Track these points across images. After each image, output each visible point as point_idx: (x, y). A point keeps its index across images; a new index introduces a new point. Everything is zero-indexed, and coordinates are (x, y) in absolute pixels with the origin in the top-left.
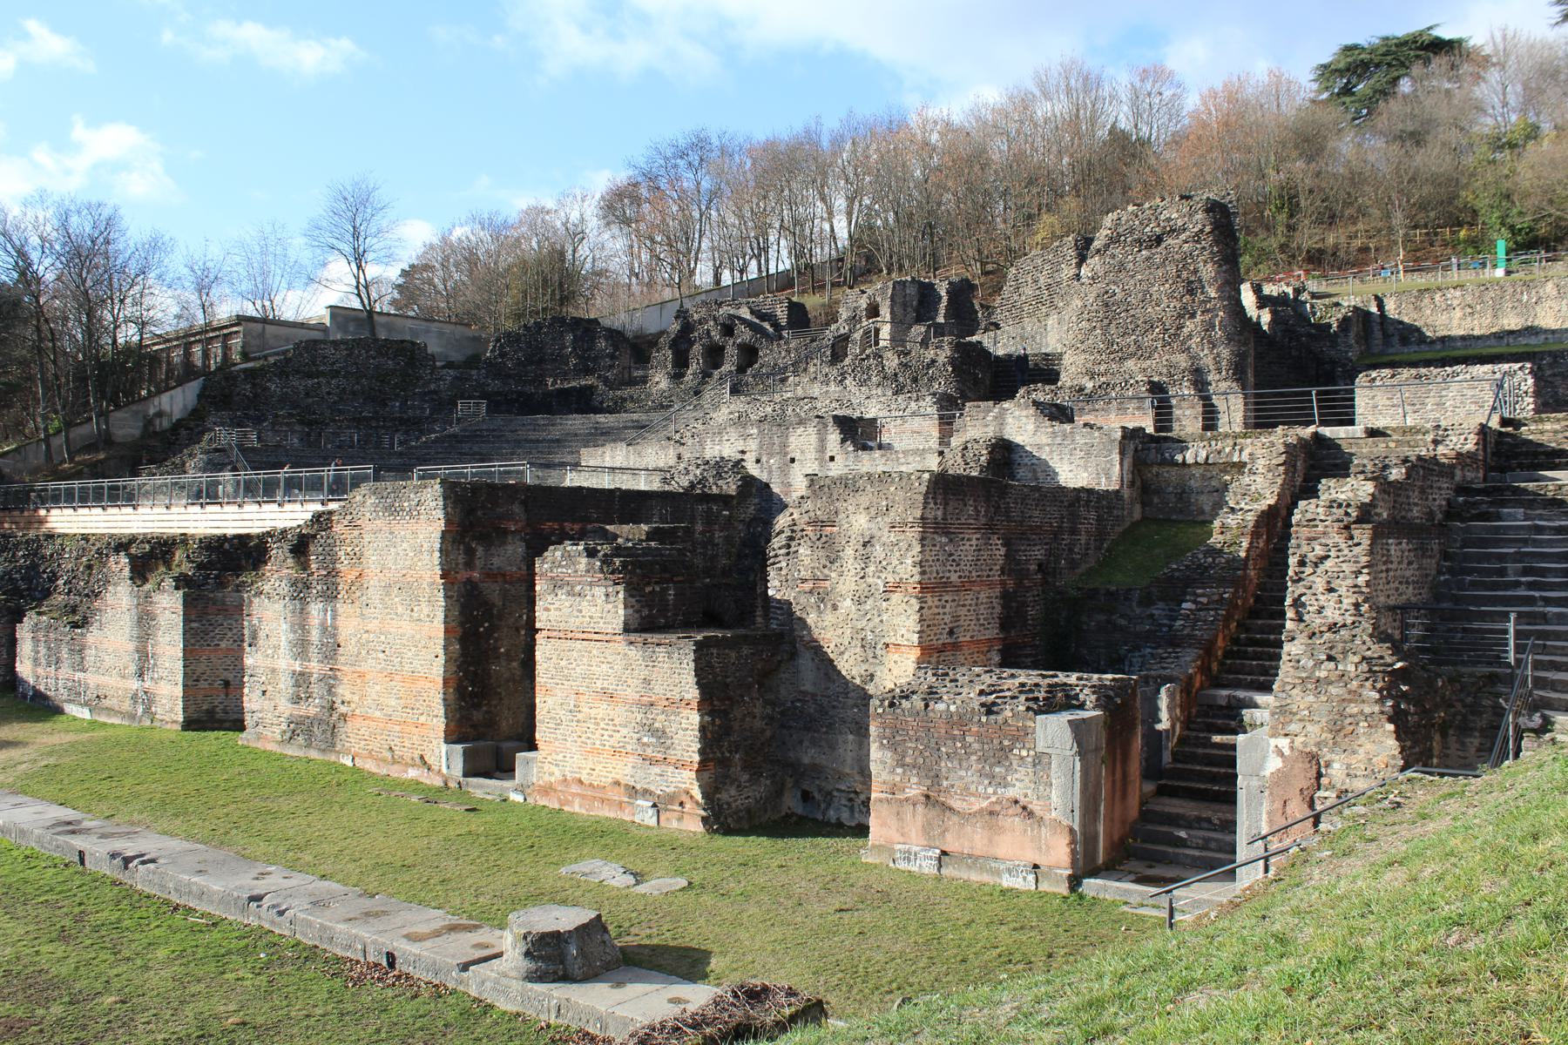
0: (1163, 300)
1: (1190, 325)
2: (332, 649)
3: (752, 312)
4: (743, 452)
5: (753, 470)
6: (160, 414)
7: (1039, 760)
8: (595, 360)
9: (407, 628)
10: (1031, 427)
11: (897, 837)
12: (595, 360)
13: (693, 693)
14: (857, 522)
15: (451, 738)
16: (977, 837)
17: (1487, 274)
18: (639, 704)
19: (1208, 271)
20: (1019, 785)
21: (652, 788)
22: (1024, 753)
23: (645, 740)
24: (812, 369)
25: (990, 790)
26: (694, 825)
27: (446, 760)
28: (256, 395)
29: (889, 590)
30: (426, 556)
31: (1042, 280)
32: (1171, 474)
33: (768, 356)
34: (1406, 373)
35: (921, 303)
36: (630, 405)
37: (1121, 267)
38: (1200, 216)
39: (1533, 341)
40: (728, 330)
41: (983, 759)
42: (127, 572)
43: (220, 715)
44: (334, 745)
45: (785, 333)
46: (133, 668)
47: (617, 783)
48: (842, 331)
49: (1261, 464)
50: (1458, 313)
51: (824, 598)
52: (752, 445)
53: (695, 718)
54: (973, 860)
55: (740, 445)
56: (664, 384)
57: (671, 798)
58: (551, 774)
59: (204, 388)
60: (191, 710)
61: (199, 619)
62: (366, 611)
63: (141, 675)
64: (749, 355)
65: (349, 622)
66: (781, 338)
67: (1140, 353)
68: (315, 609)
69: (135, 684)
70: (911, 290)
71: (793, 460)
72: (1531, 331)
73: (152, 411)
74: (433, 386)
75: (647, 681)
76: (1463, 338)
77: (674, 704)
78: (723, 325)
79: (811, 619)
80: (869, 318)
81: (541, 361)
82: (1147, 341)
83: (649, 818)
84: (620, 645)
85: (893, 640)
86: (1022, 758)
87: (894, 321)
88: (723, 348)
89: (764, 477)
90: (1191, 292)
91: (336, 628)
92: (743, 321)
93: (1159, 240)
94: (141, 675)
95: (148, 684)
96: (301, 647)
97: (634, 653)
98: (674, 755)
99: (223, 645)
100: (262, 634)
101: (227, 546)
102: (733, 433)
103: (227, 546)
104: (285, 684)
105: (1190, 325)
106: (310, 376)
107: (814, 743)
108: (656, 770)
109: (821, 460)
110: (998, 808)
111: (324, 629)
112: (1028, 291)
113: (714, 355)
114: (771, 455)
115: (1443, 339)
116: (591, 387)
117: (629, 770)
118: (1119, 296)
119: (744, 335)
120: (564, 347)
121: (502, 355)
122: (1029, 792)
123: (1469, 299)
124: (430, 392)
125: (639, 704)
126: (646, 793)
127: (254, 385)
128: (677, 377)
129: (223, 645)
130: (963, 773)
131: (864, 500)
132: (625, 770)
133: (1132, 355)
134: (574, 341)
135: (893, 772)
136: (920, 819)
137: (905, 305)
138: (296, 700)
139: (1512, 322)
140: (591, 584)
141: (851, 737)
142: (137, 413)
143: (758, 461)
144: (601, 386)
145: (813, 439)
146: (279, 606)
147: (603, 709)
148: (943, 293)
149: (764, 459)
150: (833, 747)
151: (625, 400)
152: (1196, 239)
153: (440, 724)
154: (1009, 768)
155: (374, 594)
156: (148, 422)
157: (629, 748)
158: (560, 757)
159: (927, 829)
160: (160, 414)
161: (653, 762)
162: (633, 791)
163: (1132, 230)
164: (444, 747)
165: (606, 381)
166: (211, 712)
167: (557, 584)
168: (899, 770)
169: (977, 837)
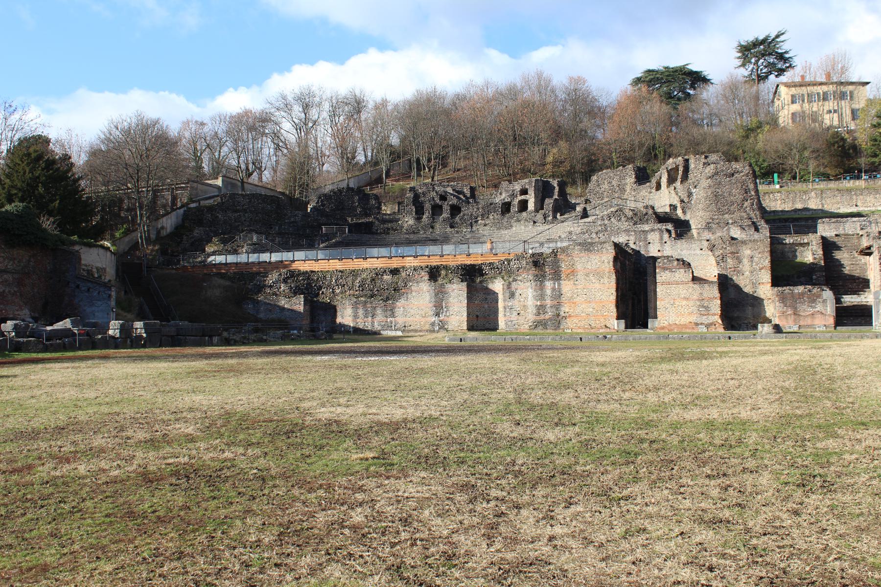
0: (737, 194)
1: (746, 204)
2: (558, 295)
3: (453, 190)
5: (632, 246)
6: (163, 228)
7: (824, 301)
8: (370, 209)
9: (597, 286)
12: (370, 209)
13: (718, 295)
14: (746, 252)
15: (618, 318)
17: (772, 187)
18: (699, 300)
19: (751, 186)
20: (819, 307)
24: (491, 217)
26: (721, 329)
27: (616, 325)
29: (762, 268)
30: (607, 264)
31: (614, 183)
32: (780, 247)
33: (466, 210)
34: (833, 220)
36: (391, 232)
37: (720, 183)
38: (747, 168)
39: (807, 213)
40: (443, 198)
42: (427, 277)
44: (559, 327)
45: (471, 200)
49: (814, 243)
50: (779, 202)
51: (739, 272)
52: (632, 239)
53: (719, 302)
54: (808, 326)
55: (627, 238)
56: (411, 222)
57: (711, 324)
63: (437, 314)
64: (455, 210)
65: (566, 287)
66: (469, 203)
67: (729, 212)
68: (549, 284)
70: (540, 184)
72: (806, 209)
73: (159, 226)
74: (292, 219)
76: (782, 211)
77: (711, 299)
78: (441, 196)
79: (734, 278)
80: (521, 195)
82: (732, 208)
83: (705, 330)
84: (691, 285)
87: (536, 197)
88: (441, 207)
89: (638, 249)
90: (746, 193)
91: (560, 290)
92: (452, 194)
93: (733, 175)
94: (437, 314)
96: (542, 297)
100: (517, 294)
102: (624, 234)
104: (532, 310)
105: (746, 204)
106: (236, 211)
109: (661, 243)
111: (553, 289)
112: (606, 186)
113: (437, 210)
115: (774, 212)
116: (372, 222)
119: (454, 201)
120: (353, 202)
121: (323, 205)
123: (783, 197)
125: (699, 300)
126: (701, 324)
128: (419, 219)
132: (694, 319)
134: (359, 200)
137: (538, 190)
138: (539, 314)
139: (799, 206)
144: (377, 222)
145: (658, 236)
146: (529, 284)
147: (684, 302)
148: (556, 185)
151: (388, 229)
152: (747, 175)
153: (615, 314)
155: (580, 276)
159: (795, 320)
160: (163, 228)
162: (697, 324)
163: (723, 171)
164: (616, 322)
165: (378, 219)
166: (473, 326)
167: (665, 269)
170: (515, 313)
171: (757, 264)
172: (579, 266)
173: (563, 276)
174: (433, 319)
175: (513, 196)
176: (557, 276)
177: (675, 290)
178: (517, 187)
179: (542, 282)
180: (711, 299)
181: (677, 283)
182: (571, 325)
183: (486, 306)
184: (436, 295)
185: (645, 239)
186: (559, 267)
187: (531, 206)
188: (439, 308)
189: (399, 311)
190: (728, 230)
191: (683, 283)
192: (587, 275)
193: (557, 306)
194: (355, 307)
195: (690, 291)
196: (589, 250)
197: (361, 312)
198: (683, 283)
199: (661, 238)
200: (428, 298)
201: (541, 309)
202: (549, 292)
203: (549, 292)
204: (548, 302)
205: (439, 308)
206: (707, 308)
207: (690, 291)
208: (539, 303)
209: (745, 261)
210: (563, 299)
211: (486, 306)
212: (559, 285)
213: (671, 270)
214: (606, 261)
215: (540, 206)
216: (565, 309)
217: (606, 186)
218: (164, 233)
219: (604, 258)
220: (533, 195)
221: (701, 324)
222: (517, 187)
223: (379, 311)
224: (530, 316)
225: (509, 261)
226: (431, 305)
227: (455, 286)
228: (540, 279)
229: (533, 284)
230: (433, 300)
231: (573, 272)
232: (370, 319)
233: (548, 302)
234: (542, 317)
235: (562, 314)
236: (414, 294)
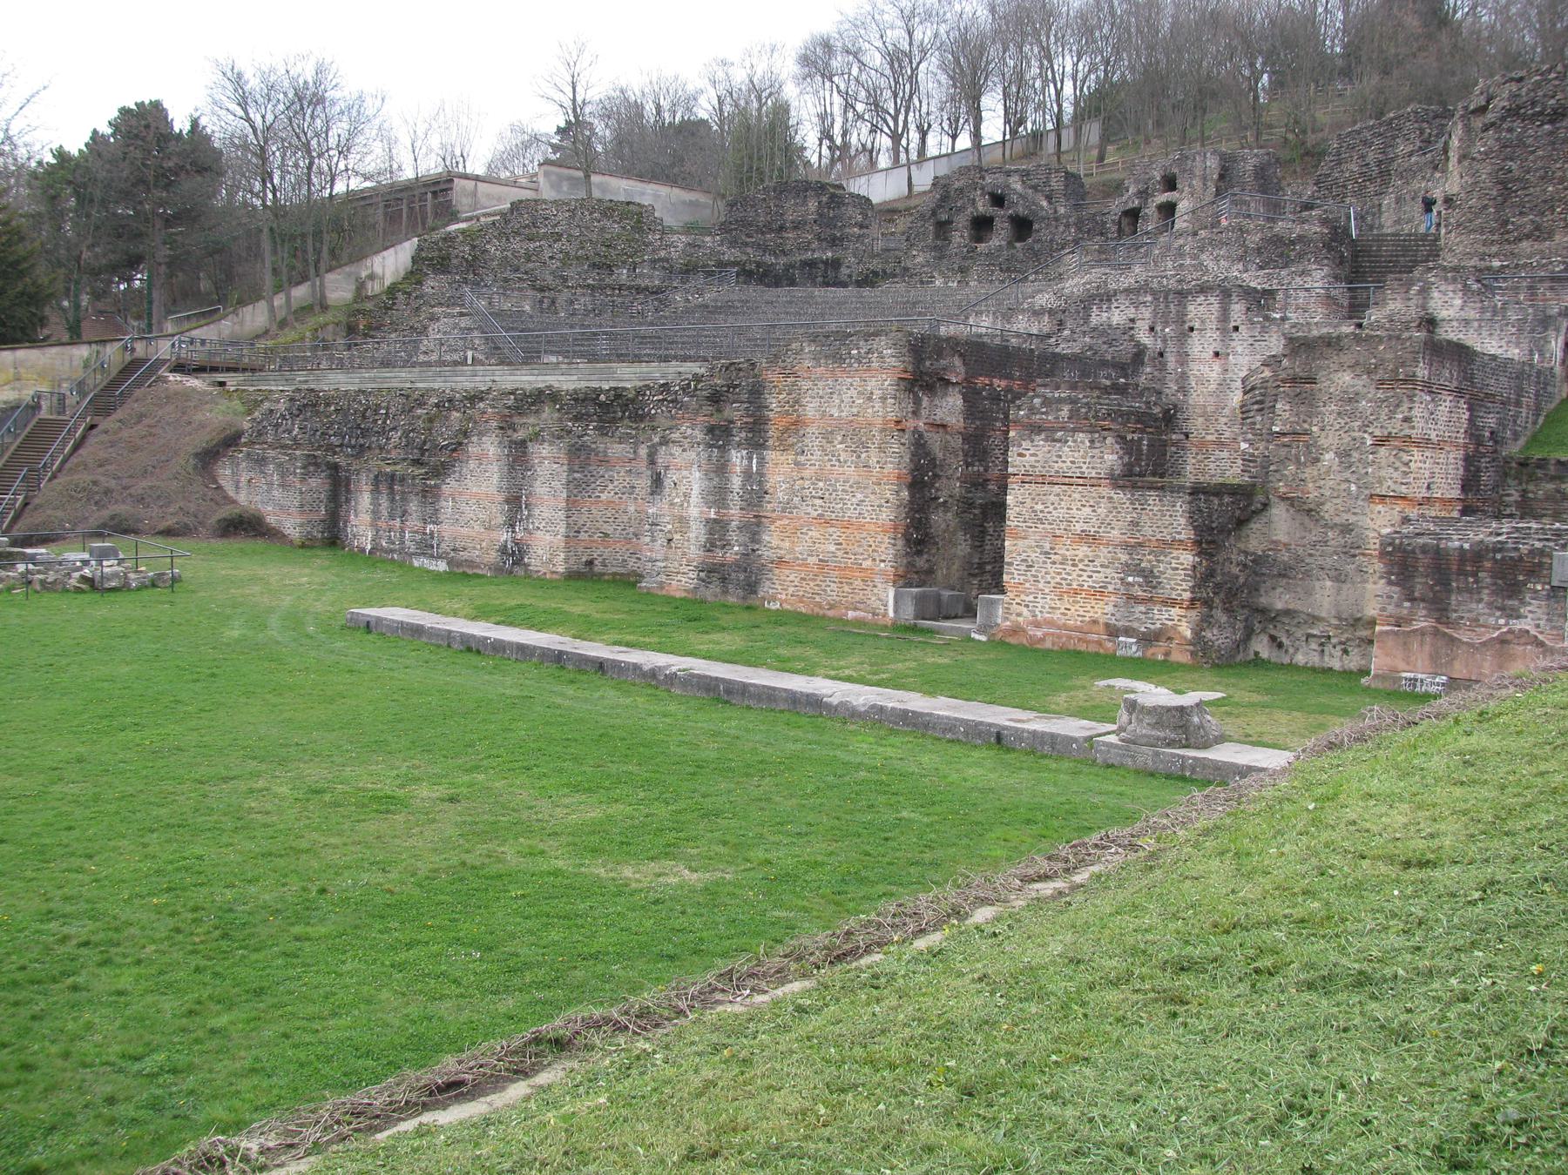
2: (756, 494)
4: (1132, 320)
6: (372, 277)
10: (1458, 302)
11: (1401, 665)
13: (1187, 534)
16: (1486, 664)
18: (1126, 546)
21: (1135, 625)
22: (1539, 587)
23: (1130, 579)
25: (1502, 621)
28: (475, 258)
30: (878, 405)
35: (1222, 177)
41: (1493, 593)
43: (598, 568)
46: (501, 519)
47: (1095, 622)
48: (1131, 205)
52: (1147, 313)
55: (1131, 312)
58: (1019, 615)
59: (420, 249)
60: (572, 561)
61: (582, 468)
62: (802, 459)
65: (779, 468)
68: (737, 458)
69: (504, 536)
71: (1192, 329)
73: (364, 274)
74: (663, 254)
75: (1135, 524)
77: (1166, 545)
81: (782, 228)
85: (1378, 491)
86: (1536, 591)
91: (762, 475)
96: (718, 496)
97: (1120, 496)
98: (1165, 592)
99: (604, 497)
100: (668, 483)
101: (603, 398)
103: (603, 398)
104: (697, 532)
107: (1287, 589)
108: (1142, 608)
109: (1224, 331)
110: (1509, 637)
111: (747, 475)
114: (1166, 324)
117: (1110, 609)
118: (1516, 173)
122: (1542, 623)
124: (660, 260)
125: (1126, 546)
127: (474, 247)
129: (604, 497)
130: (1474, 606)
131: (1347, 358)
132: (1103, 610)
133: (1528, 237)
135: (1398, 605)
136: (1427, 648)
138: (710, 546)
140: (1074, 430)
141: (1328, 583)
142: (349, 275)
143: (1152, 329)
147: (1083, 551)
149: (1158, 328)
150: (1309, 593)
154: (1523, 602)
155: (813, 440)
156: (361, 286)
157: (1111, 588)
158: (1031, 598)
159: (1434, 658)
160: (372, 277)
161: (1138, 601)
162: (1113, 632)
167: (1036, 429)
168: (1407, 604)
169: (1486, 664)
170: (661, 541)
171: (1364, 428)
172: (810, 409)
173: (772, 432)
175: (1144, 194)
176: (757, 440)
179: (723, 449)
180: (1166, 545)
181: (1067, 481)
182: (782, 591)
183: (632, 509)
184: (512, 468)
185: (1181, 318)
188: (516, 504)
190: (1425, 291)
191: (1085, 481)
192: (827, 436)
193: (754, 529)
195: (1102, 511)
196: (838, 359)
197: (384, 502)
198: (1085, 481)
199: (1225, 316)
200: (495, 479)
201: (717, 530)
202: (736, 482)
203: (736, 482)
204: (735, 512)
205: (516, 504)
206: (1149, 577)
207: (1102, 511)
211: (632, 509)
212: (762, 462)
214: (877, 394)
216: (774, 541)
218: (374, 288)
219: (872, 384)
221: (1128, 632)
223: (413, 506)
226: (500, 498)
229: (704, 455)
230: (504, 484)
231: (796, 425)
232: (397, 522)
235: (766, 554)
236: (472, 464)
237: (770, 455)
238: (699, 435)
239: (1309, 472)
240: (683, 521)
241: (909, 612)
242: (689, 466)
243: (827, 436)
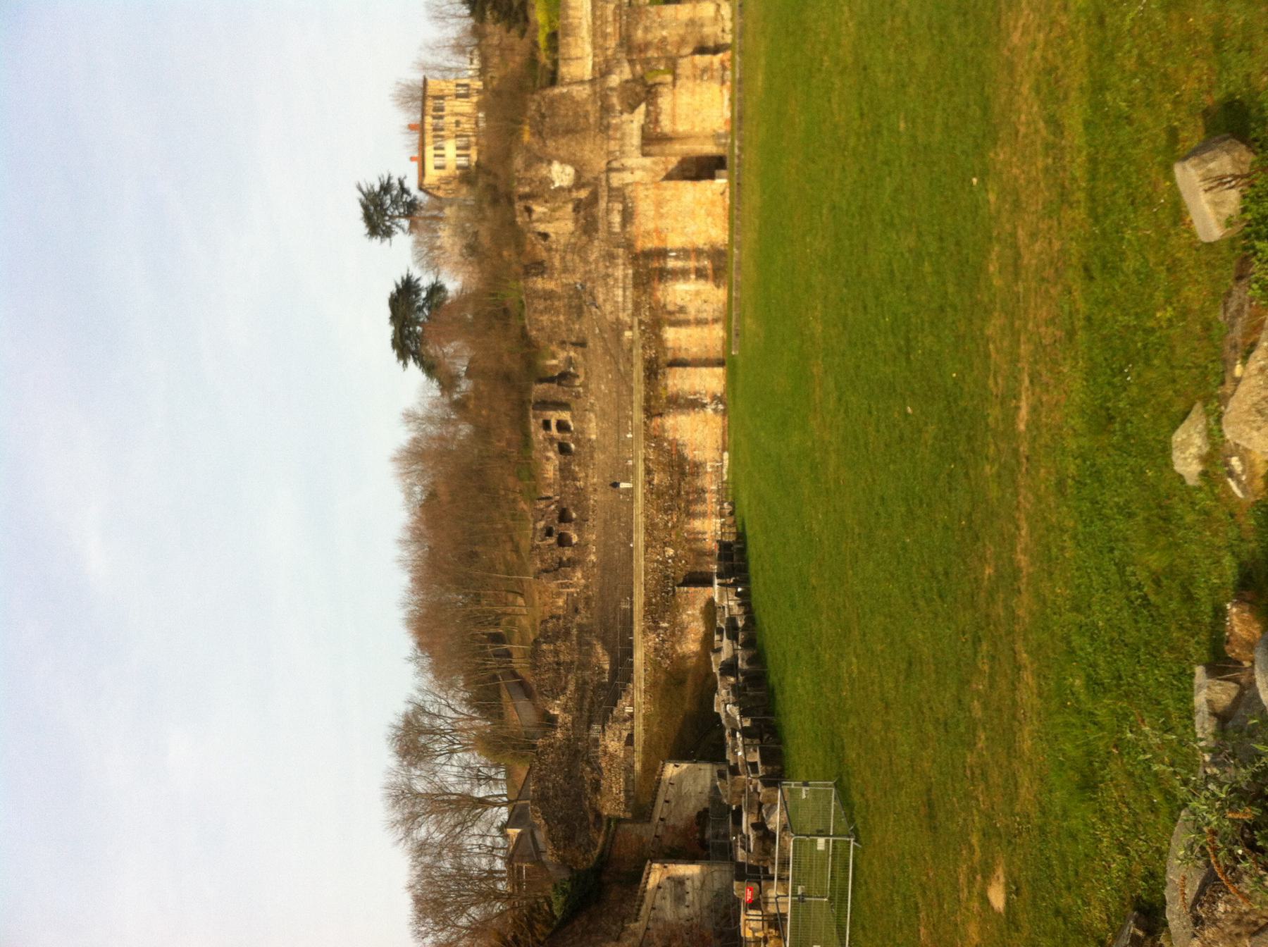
2: (684, 253)
42: (659, 420)
63: (704, 406)
68: (671, 264)
75: (687, 78)
91: (677, 250)
94: (704, 406)
95: (707, 400)
96: (683, 274)
111: (677, 258)
146: (670, 289)
170: (705, 306)
172: (651, 226)
173: (662, 246)
174: (709, 410)
176: (662, 253)
177: (682, 110)
178: (541, 434)
181: (673, 109)
186: (650, 250)
187: (565, 416)
188: (692, 404)
189: (699, 456)
192: (662, 216)
193: (698, 253)
194: (692, 516)
197: (699, 508)
199: (617, 170)
201: (700, 274)
202: (680, 264)
204: (692, 264)
205: (692, 404)
206: (704, 71)
208: (693, 277)
209: (650, 37)
210: (689, 246)
212: (671, 251)
213: (658, 114)
215: (563, 406)
216: (700, 242)
217: (545, 319)
220: (551, 413)
221: (722, 77)
222: (539, 435)
224: (706, 287)
225: (641, 322)
227: (670, 382)
228: (664, 275)
229: (670, 283)
233: (692, 264)
234: (710, 272)
236: (678, 437)
237: (669, 246)
238: (662, 287)
239: (670, 40)
240: (698, 293)
241: (723, 172)
242: (674, 291)
243: (662, 216)
